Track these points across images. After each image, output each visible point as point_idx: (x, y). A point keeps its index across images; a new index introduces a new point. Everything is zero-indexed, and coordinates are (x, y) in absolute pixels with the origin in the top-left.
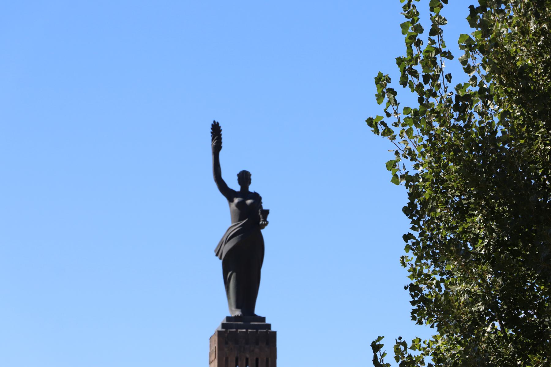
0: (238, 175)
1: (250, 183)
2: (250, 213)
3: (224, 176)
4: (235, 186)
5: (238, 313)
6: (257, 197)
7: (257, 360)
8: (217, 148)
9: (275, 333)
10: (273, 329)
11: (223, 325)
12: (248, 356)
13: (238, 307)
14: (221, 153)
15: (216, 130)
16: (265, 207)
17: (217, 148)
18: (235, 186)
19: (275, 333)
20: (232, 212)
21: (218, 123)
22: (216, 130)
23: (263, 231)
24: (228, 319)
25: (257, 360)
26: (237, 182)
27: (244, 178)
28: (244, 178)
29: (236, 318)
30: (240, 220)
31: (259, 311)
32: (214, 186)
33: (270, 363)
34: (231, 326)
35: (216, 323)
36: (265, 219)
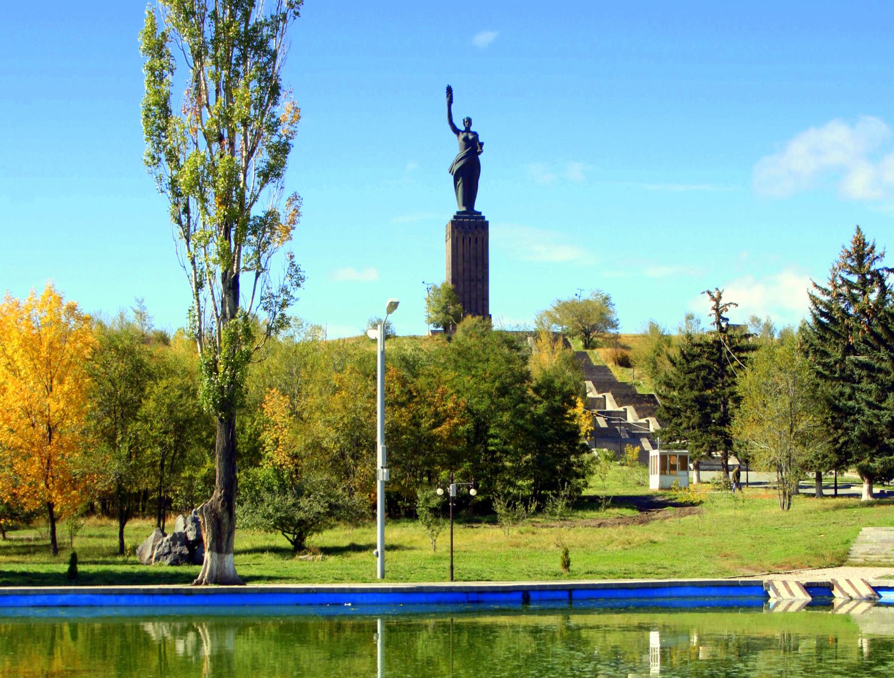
2: (473, 147)
5: (464, 209)
6: (475, 134)
8: (450, 102)
10: (486, 219)
11: (455, 217)
13: (464, 205)
14: (453, 106)
15: (449, 90)
16: (481, 141)
17: (450, 102)
20: (460, 144)
22: (449, 90)
23: (480, 157)
24: (458, 213)
27: (469, 122)
29: (463, 212)
30: (466, 149)
31: (477, 208)
34: (460, 218)
35: (450, 217)
36: (481, 148)
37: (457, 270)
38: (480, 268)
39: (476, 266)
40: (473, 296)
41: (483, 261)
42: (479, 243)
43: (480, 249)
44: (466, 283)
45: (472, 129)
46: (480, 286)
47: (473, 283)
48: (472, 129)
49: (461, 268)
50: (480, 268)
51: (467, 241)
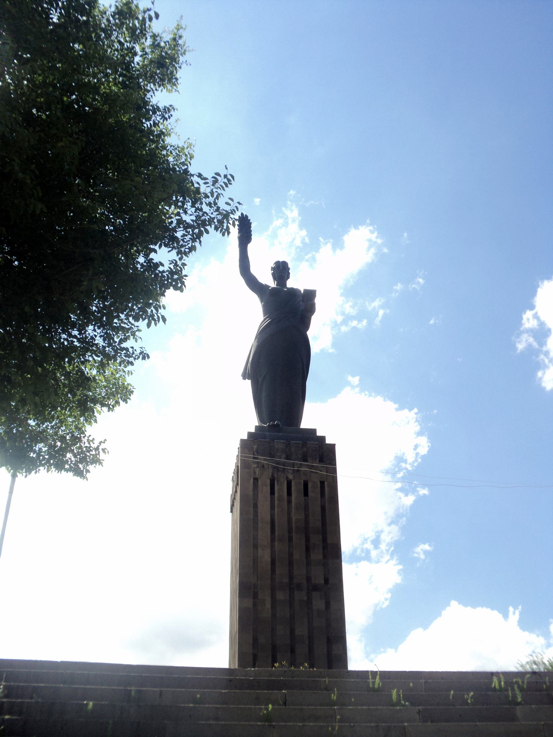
0: (273, 269)
1: (288, 277)
3: (254, 270)
4: (267, 279)
7: (306, 485)
9: (334, 446)
12: (291, 477)
14: (250, 246)
18: (267, 279)
19: (334, 446)
21: (247, 216)
25: (306, 485)
26: (270, 272)
27: (281, 271)
28: (281, 271)
29: (273, 428)
32: (241, 281)
33: (326, 489)
37: (255, 560)
38: (317, 555)
39: (308, 549)
40: (301, 631)
41: (325, 540)
42: (314, 492)
43: (315, 508)
44: (281, 596)
45: (290, 284)
46: (318, 604)
47: (300, 596)
48: (290, 284)
49: (265, 555)
50: (317, 555)
51: (281, 489)
